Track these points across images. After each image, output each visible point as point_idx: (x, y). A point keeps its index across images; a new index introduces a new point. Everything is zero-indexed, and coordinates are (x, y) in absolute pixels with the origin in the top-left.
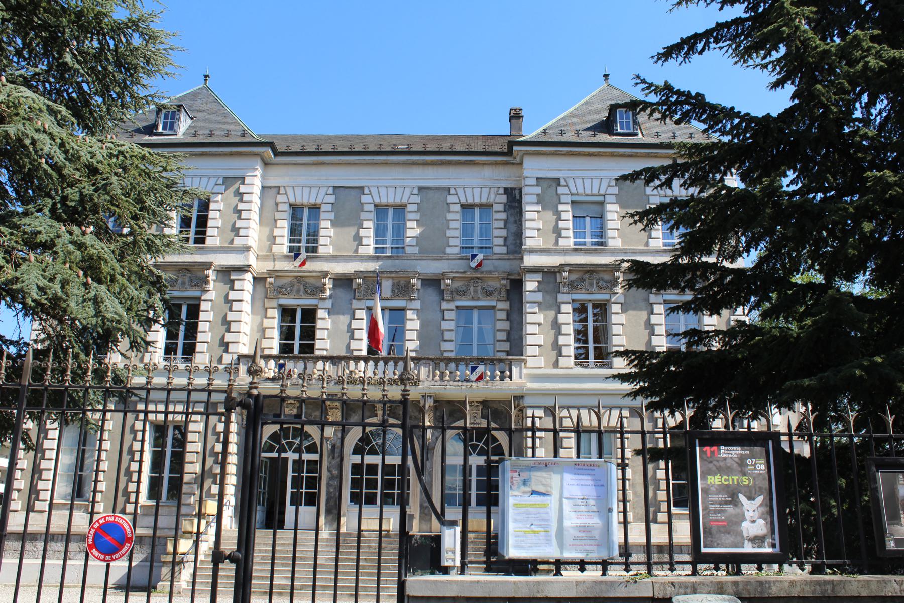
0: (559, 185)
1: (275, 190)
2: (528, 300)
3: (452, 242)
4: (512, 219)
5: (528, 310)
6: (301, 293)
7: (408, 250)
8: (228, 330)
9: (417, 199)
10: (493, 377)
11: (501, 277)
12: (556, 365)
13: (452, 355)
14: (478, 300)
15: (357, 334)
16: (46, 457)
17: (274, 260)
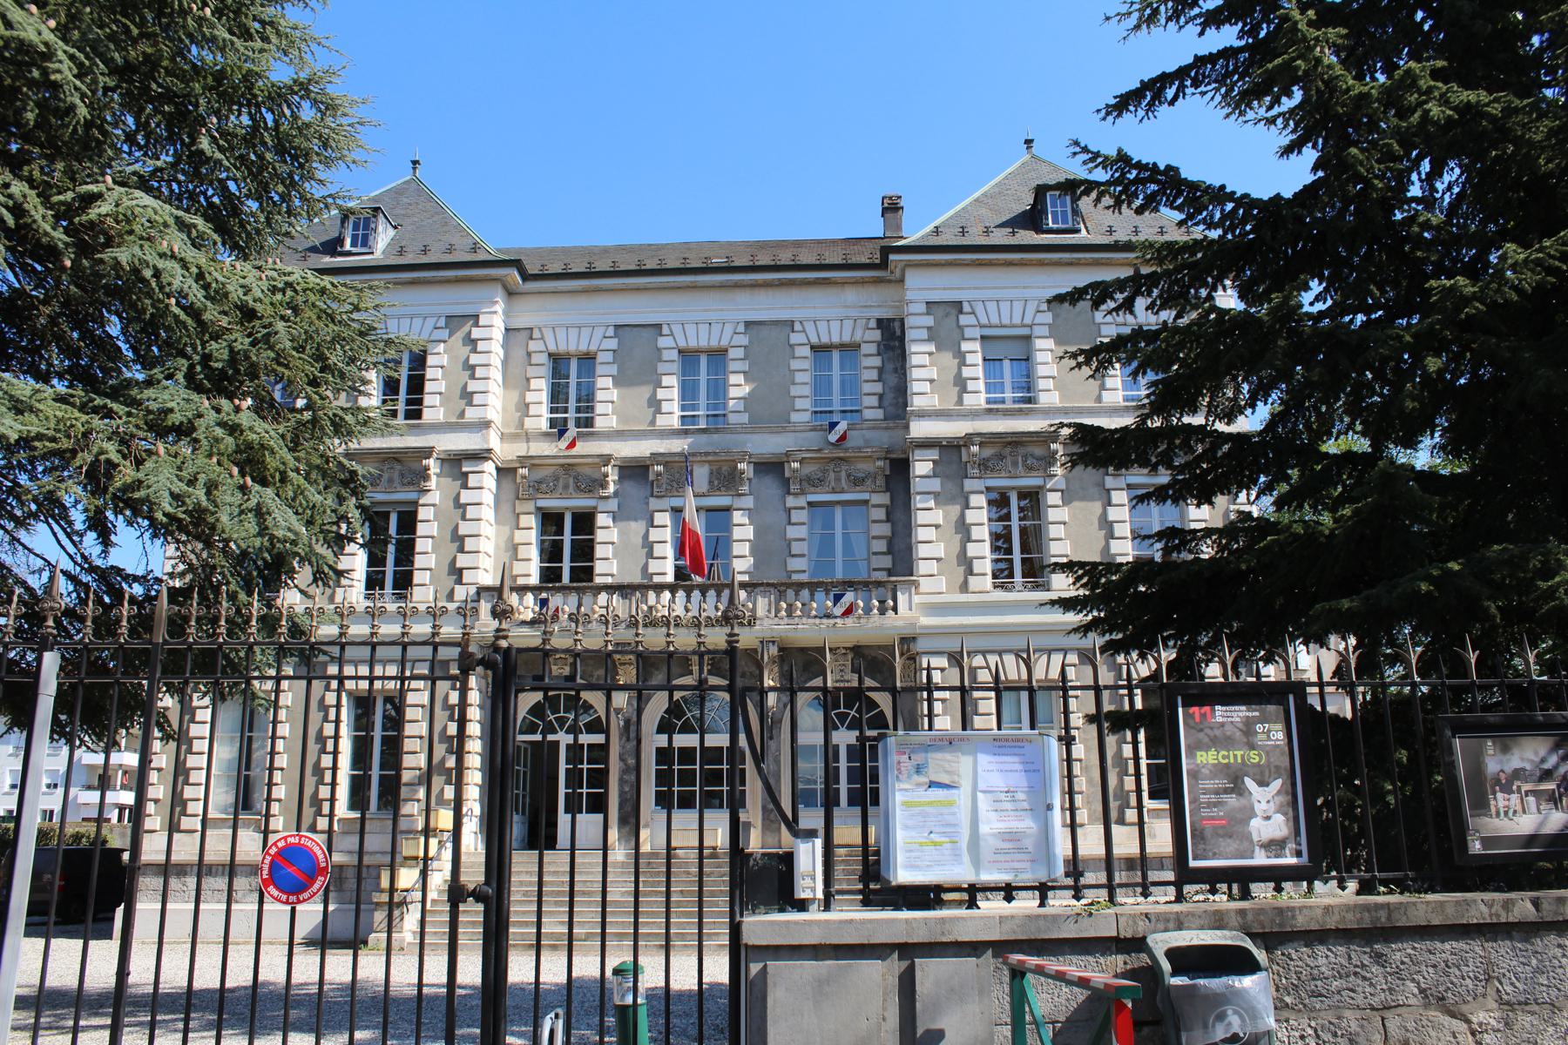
0: (961, 312)
1: (525, 334)
3: (799, 404)
4: (890, 366)
5: (919, 505)
6: (571, 490)
7: (732, 418)
8: (461, 550)
9: (744, 340)
10: (868, 610)
11: (876, 455)
12: (964, 588)
13: (804, 578)
14: (842, 491)
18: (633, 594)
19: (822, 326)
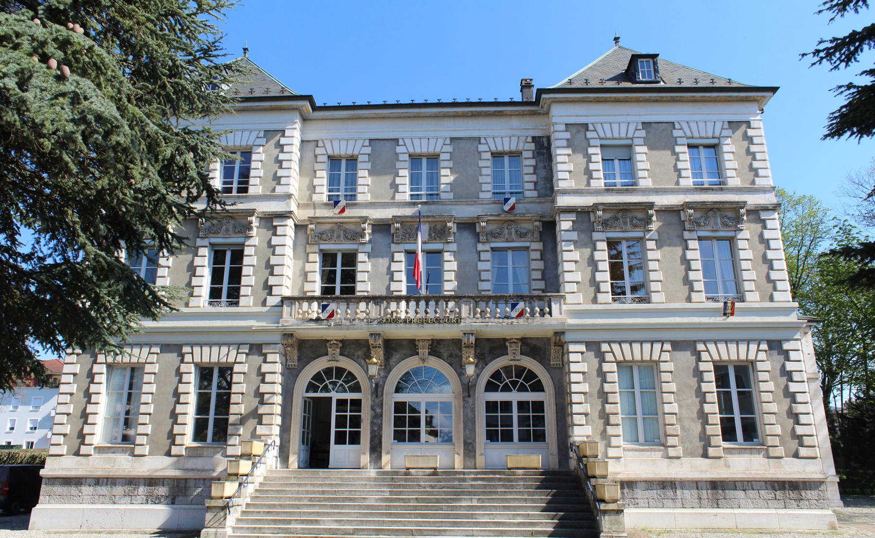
0: (587, 130)
1: (314, 144)
2: (563, 239)
3: (485, 187)
4: (541, 165)
5: (564, 248)
6: (342, 238)
8: (272, 274)
9: (449, 149)
10: (533, 314)
11: (534, 218)
12: (595, 300)
13: (490, 293)
14: (513, 241)
15: (396, 276)
16: (92, 401)
17: (315, 208)
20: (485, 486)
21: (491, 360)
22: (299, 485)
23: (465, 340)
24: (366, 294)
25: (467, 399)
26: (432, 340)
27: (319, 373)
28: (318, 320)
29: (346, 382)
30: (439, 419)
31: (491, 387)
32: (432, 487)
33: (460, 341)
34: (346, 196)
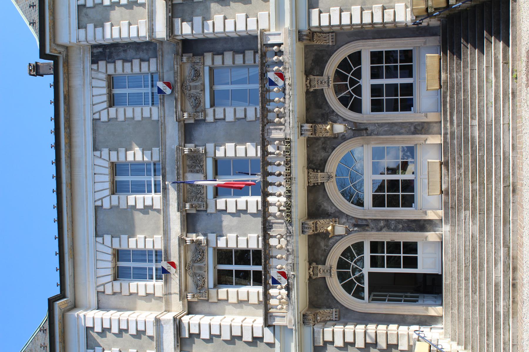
0: (84, 6)
1: (101, 296)
2: (201, 32)
3: (146, 114)
4: (122, 55)
5: (211, 30)
6: (202, 265)
7: (156, 158)
8: (240, 338)
9: (105, 151)
10: (280, 63)
11: (180, 62)
13: (259, 108)
14: (203, 84)
17: (170, 294)
18: (269, 222)
19: (96, 100)
20: (459, 112)
21: (329, 107)
22: (459, 304)
23: (308, 134)
24: (260, 239)
25: (369, 132)
26: (308, 168)
27: (344, 286)
28: (288, 288)
29: (352, 257)
30: (389, 161)
31: (356, 107)
32: (460, 167)
33: (309, 140)
34: (157, 261)
